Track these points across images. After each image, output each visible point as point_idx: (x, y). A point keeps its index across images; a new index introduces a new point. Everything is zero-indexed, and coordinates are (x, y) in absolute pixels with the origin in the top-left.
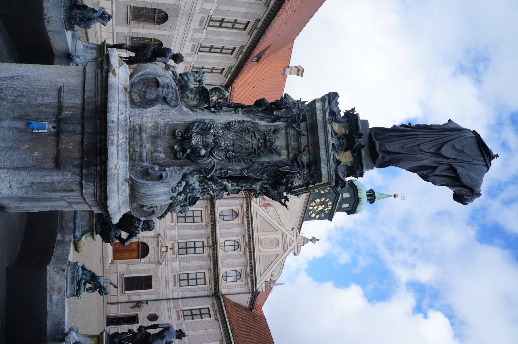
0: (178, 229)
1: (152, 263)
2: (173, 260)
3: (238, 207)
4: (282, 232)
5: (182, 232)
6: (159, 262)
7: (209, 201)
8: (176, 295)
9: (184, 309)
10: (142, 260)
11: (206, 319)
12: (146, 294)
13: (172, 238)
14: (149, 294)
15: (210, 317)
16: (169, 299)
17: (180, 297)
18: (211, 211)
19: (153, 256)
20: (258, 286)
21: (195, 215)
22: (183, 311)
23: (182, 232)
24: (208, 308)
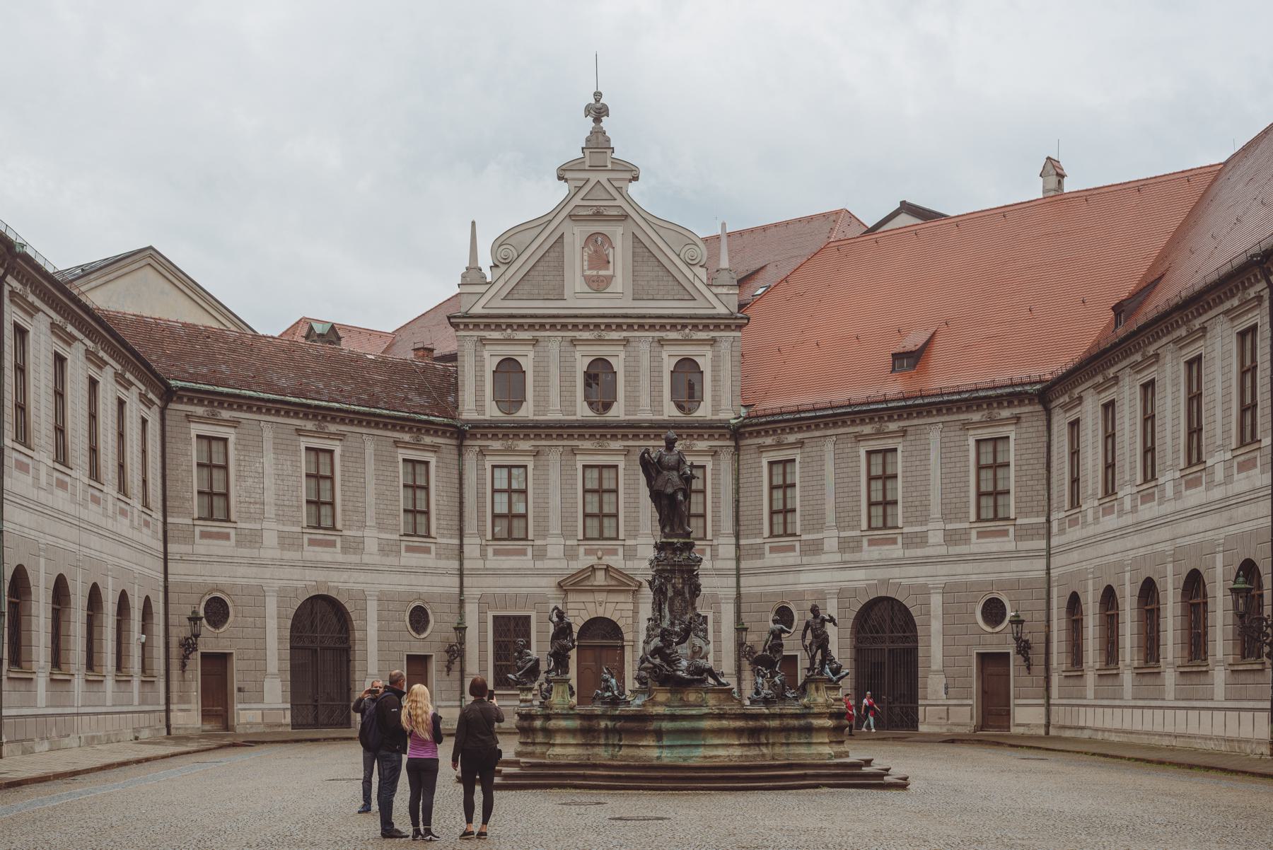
0: (545, 537)
1: (636, 612)
2: (630, 554)
3: (486, 354)
4: (568, 223)
5: (555, 525)
6: (634, 592)
7: (467, 442)
8: (731, 551)
9: (766, 533)
10: (626, 637)
11: (797, 475)
12: (717, 631)
13: (570, 554)
14: (717, 622)
15: (794, 460)
16: (738, 569)
17: (733, 541)
18: (495, 436)
19: (619, 606)
20: (722, 310)
21: (505, 486)
22: (772, 535)
23: (555, 525)
24: (771, 464)
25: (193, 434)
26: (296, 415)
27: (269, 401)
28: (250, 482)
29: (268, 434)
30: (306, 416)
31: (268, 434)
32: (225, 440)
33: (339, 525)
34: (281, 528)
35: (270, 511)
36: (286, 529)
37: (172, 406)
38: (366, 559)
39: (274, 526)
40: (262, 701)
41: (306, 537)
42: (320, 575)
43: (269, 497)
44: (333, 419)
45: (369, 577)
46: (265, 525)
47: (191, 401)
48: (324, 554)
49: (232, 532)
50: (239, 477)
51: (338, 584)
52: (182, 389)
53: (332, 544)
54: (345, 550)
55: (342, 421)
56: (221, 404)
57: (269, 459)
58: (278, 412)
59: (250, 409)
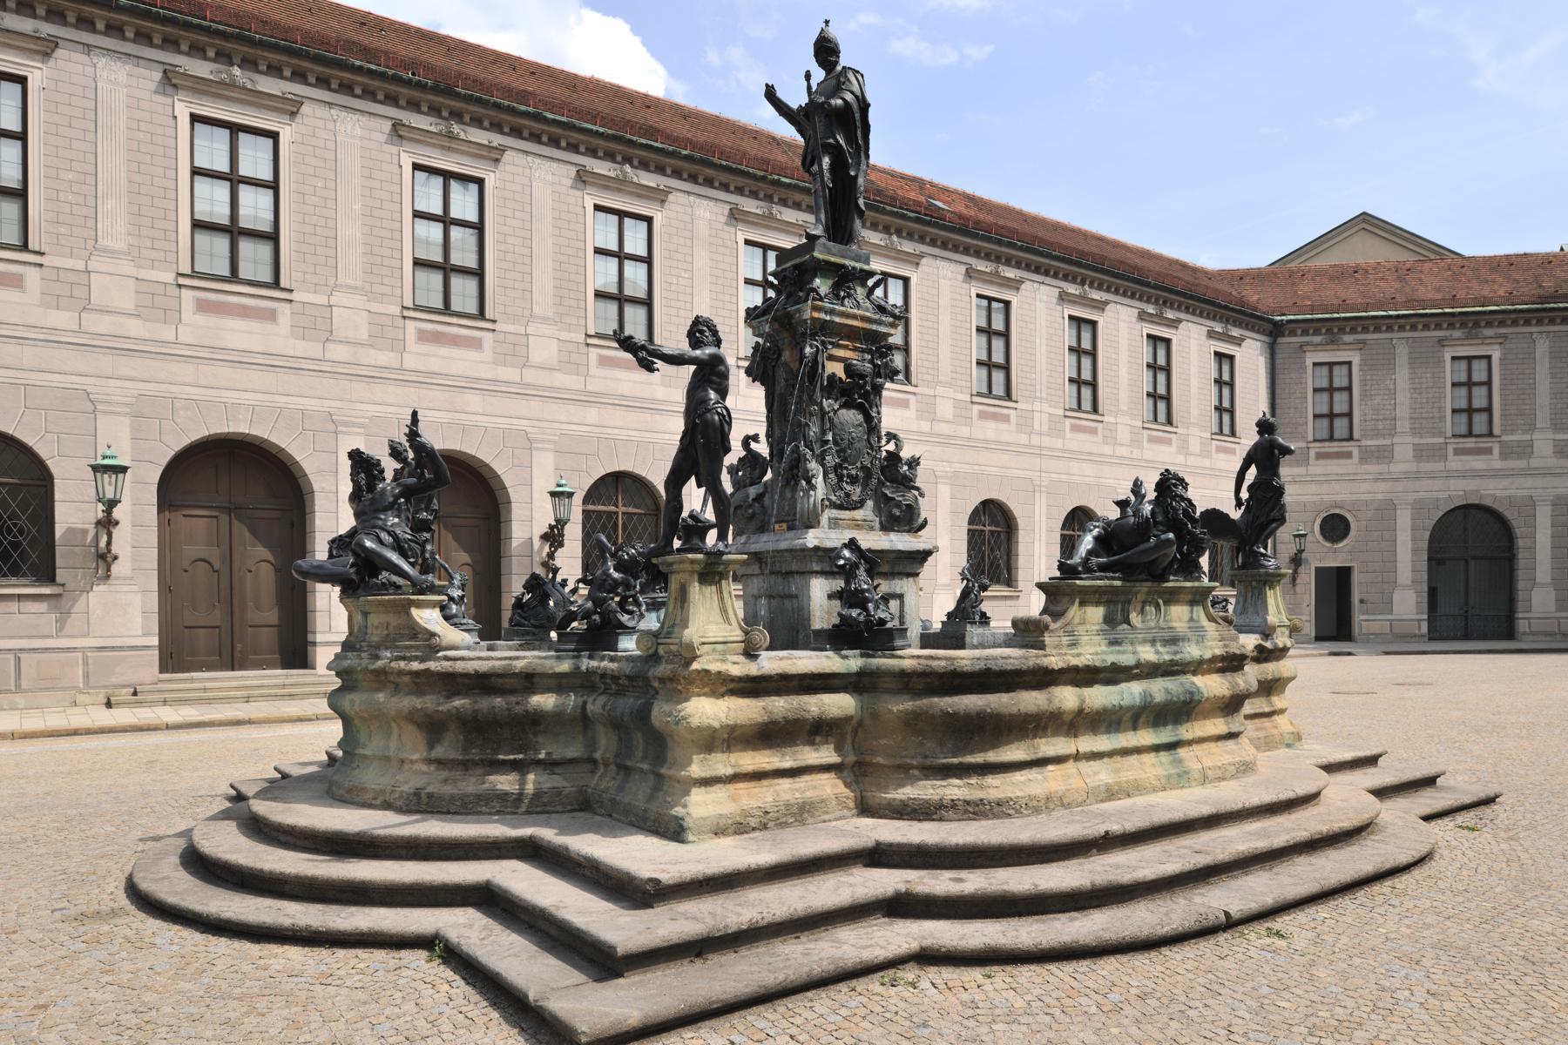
25: (1309, 361)
26: (1438, 327)
27: (1398, 317)
28: (1377, 400)
29: (1402, 352)
30: (1451, 326)
31: (1402, 352)
32: (1349, 363)
33: (1496, 431)
34: (1417, 441)
35: (1403, 425)
36: (1425, 441)
37: (1280, 340)
38: (1535, 463)
39: (1409, 439)
40: (1391, 612)
41: (1450, 449)
42: (1470, 485)
43: (1403, 412)
44: (1489, 324)
45: (1539, 482)
46: (1396, 440)
47: (1305, 332)
48: (1477, 463)
49: (1356, 452)
50: (1365, 396)
51: (1492, 491)
52: (1289, 322)
53: (1489, 451)
54: (1504, 456)
55: (1502, 324)
56: (1342, 330)
57: (1402, 377)
58: (1414, 328)
59: (1377, 330)
